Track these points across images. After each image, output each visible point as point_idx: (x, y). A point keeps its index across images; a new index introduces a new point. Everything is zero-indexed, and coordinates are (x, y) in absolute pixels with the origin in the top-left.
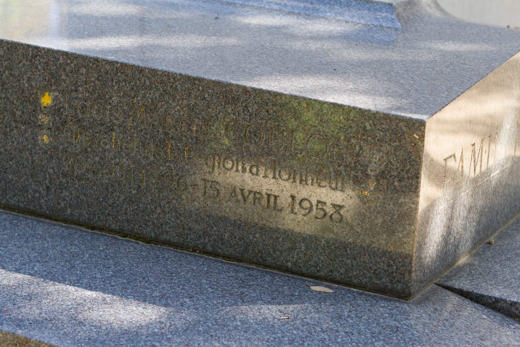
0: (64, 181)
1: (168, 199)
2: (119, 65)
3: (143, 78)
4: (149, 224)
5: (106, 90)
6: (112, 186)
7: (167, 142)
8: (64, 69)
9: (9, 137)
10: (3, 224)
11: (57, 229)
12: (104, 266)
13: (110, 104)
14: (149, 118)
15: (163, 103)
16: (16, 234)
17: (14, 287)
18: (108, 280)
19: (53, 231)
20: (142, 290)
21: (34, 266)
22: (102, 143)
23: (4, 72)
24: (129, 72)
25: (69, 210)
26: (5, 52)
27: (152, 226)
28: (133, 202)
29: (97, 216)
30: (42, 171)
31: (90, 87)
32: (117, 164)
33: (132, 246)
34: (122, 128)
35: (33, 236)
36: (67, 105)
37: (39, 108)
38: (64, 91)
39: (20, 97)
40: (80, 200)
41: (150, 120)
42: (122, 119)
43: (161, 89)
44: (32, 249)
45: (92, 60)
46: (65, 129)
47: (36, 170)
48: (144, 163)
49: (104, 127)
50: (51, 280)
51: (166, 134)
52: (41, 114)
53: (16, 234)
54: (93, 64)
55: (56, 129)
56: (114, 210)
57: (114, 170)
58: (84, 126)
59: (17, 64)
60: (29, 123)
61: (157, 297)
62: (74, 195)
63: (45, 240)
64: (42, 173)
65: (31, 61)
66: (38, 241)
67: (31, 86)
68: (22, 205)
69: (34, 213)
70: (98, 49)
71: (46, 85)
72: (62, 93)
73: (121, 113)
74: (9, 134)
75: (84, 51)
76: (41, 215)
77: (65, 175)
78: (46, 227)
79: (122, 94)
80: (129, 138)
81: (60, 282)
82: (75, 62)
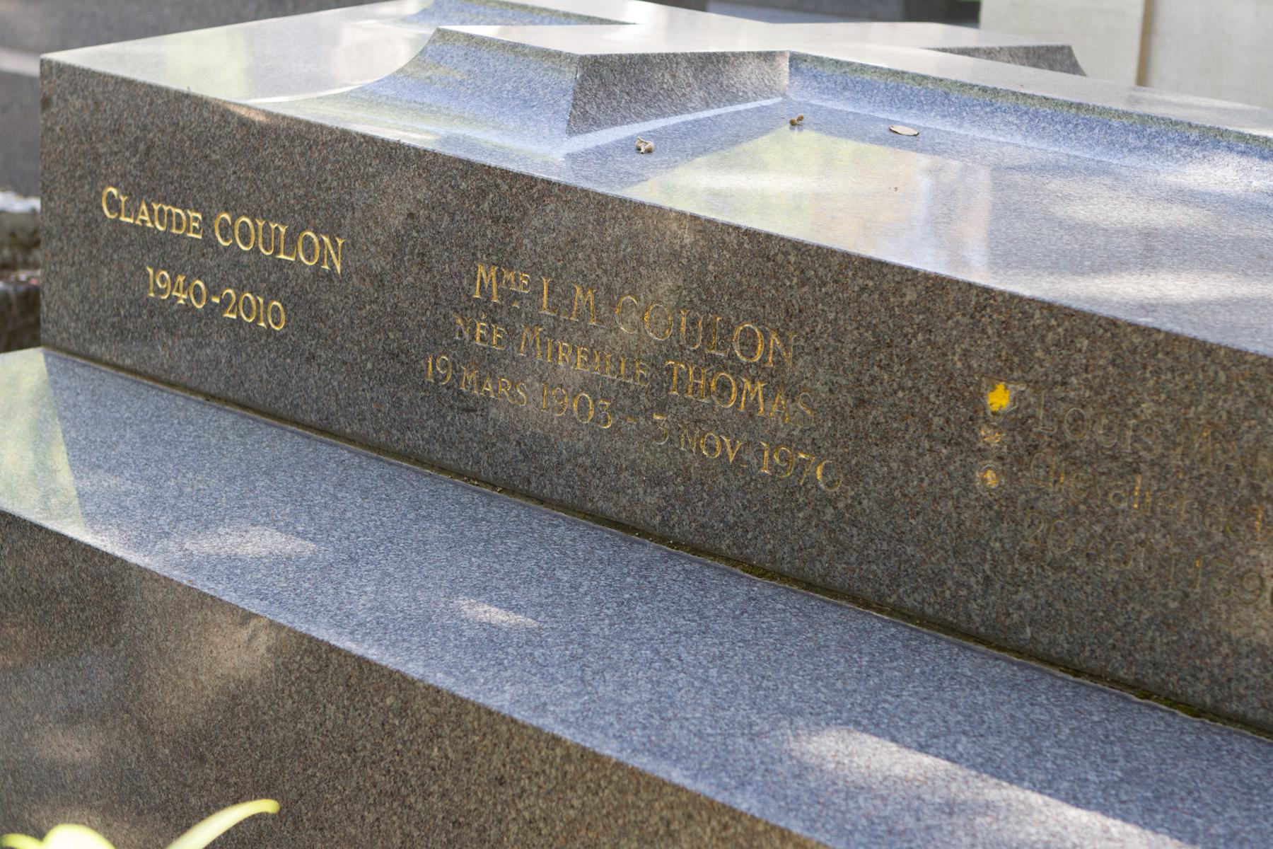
0: (1023, 568)
1: (1249, 626)
2: (1162, 336)
3: (1213, 368)
4: (1201, 676)
5: (1130, 386)
6: (1127, 588)
7: (1255, 506)
8: (1043, 338)
9: (914, 470)
10: (891, 646)
11: (1002, 668)
12: (1103, 757)
13: (1135, 416)
14: (1219, 452)
15: (1253, 422)
16: (917, 670)
17: (917, 783)
18: (1113, 788)
19: (993, 672)
20: (1187, 817)
21: (957, 741)
22: (1111, 496)
23: (915, 336)
24: (1184, 353)
25: (1028, 630)
26: (919, 295)
27: (1207, 682)
28: (1169, 626)
29: (1088, 648)
30: (977, 543)
31: (1095, 377)
32: (1142, 543)
33: (1162, 718)
34: (1157, 469)
35: (952, 678)
36: (1042, 412)
37: (981, 415)
38: (1037, 382)
39: (944, 388)
40: (1053, 612)
41: (1221, 457)
42: (1159, 450)
43: (1252, 394)
44: (952, 706)
45: (1103, 322)
46: (1034, 462)
47: (966, 540)
48: (1200, 545)
49: (1119, 464)
50: (993, 775)
51: (1255, 488)
52: (985, 427)
53: (917, 670)
54: (1106, 331)
55: (1014, 462)
56: (1127, 639)
57: (1133, 555)
58: (1075, 458)
59: (942, 321)
60: (958, 444)
61: (1219, 836)
62: (1043, 601)
63: (978, 688)
64: (977, 549)
65: (972, 317)
66: (963, 690)
67: (970, 367)
68: (929, 611)
69: (954, 630)
70: (1115, 299)
71: (1001, 369)
72: (1033, 387)
73: (1157, 438)
74: (915, 462)
75: (1087, 302)
76: (966, 635)
77: (1026, 557)
78: (979, 661)
79: (1163, 396)
80: (1172, 491)
81: (1011, 782)
82: (1067, 324)
